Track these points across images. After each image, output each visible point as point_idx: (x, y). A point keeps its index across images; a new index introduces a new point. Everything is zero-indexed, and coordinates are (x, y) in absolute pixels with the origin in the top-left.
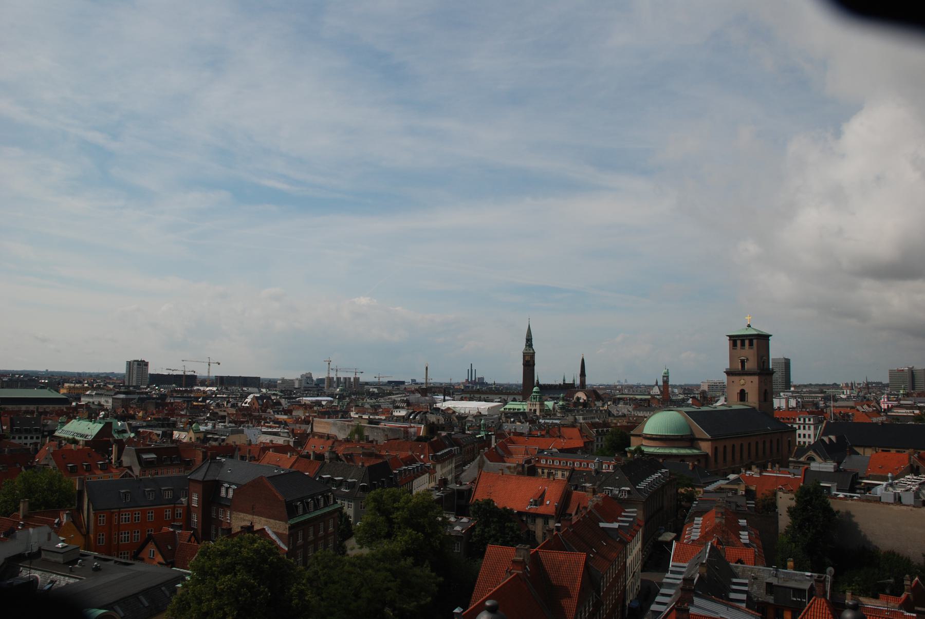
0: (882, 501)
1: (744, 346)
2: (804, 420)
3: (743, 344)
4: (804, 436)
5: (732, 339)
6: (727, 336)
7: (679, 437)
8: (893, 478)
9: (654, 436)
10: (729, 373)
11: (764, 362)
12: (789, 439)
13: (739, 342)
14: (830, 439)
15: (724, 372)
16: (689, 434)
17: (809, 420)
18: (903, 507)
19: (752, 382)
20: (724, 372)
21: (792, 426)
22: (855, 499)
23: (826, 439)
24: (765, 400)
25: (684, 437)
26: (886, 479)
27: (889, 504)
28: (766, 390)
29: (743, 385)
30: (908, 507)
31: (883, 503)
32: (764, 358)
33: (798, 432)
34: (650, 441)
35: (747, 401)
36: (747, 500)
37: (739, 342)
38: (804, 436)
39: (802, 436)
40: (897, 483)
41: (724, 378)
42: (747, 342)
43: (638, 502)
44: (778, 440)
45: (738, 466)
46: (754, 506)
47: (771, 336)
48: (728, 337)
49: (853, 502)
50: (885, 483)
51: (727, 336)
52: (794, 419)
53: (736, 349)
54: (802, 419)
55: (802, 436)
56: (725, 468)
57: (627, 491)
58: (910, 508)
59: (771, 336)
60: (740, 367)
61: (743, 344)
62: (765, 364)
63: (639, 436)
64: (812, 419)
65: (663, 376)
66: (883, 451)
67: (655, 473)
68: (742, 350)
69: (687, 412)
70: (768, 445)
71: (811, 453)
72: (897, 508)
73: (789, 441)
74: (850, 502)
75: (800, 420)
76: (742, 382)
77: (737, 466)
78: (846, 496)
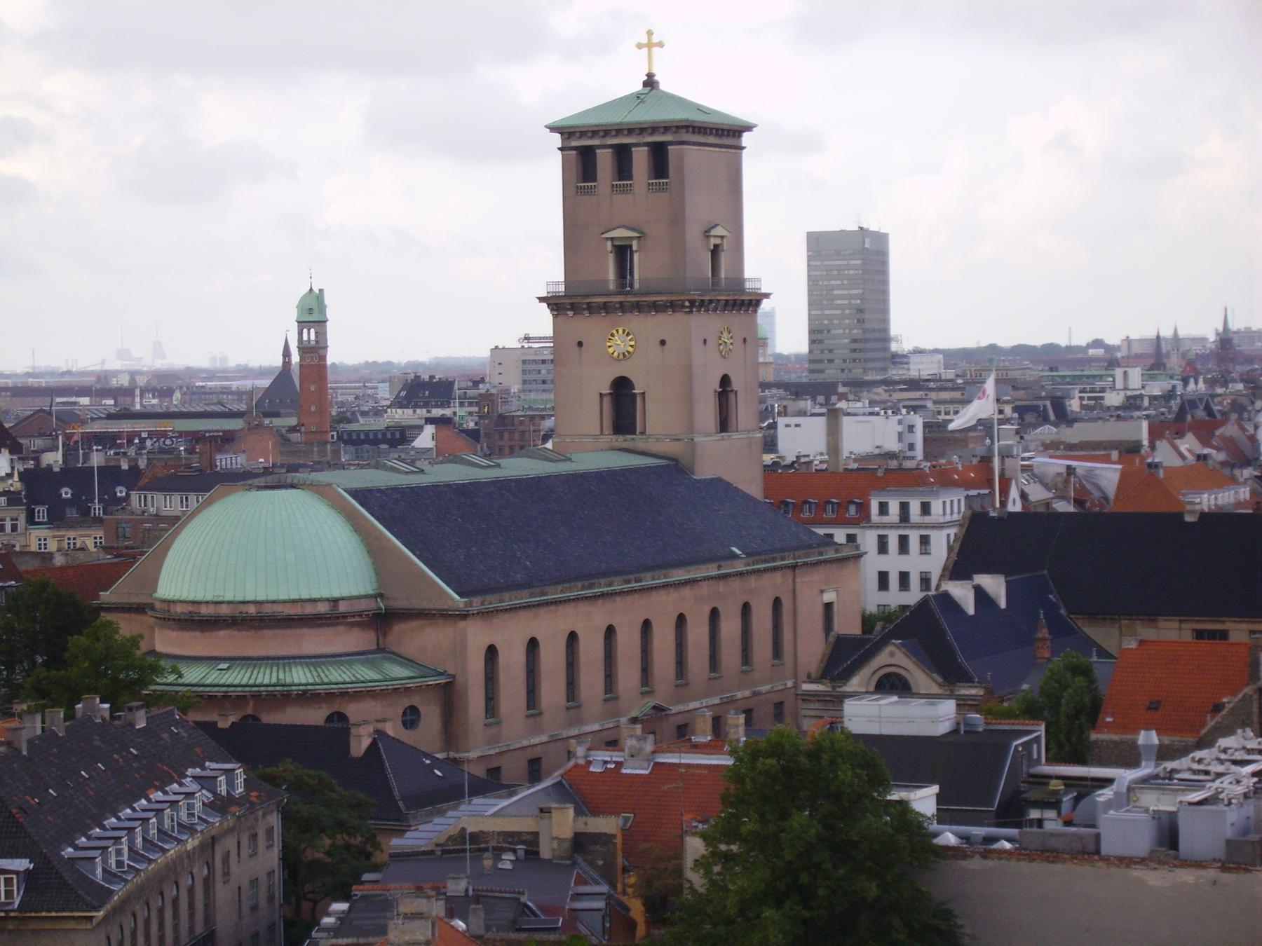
0: (1106, 849)
1: (630, 178)
2: (904, 507)
3: (623, 166)
4: (904, 578)
5: (574, 143)
6: (553, 129)
7: (322, 608)
8: (1164, 753)
9: (204, 610)
10: (555, 304)
11: (715, 251)
12: (829, 597)
13: (605, 160)
14: (981, 595)
15: (541, 300)
16: (371, 592)
17: (926, 508)
18: (1188, 876)
19: (663, 343)
20: (541, 300)
21: (851, 538)
22: (1005, 851)
23: (962, 593)
24: (724, 424)
25: (343, 607)
26: (1130, 758)
27: (1126, 861)
28: (725, 381)
29: (625, 356)
30: (1201, 872)
31: (1106, 860)
32: (719, 231)
33: (873, 563)
34: (187, 635)
35: (643, 433)
36: (580, 881)
37: (605, 160)
38: (904, 578)
39: (894, 581)
40: (1174, 771)
41: (542, 323)
42: (641, 159)
43: (71, 925)
44: (777, 603)
45: (596, 727)
46: (600, 904)
47: (749, 128)
48: (557, 139)
49: (990, 863)
50: (1125, 776)
51: (553, 129)
52: (864, 508)
53: (589, 192)
54: (894, 508)
55: (894, 581)
56: (536, 740)
57: (17, 873)
58: (1211, 874)
59: (749, 128)
60: (611, 275)
61: (623, 166)
62: (724, 258)
63: (140, 609)
64: (936, 507)
65: (302, 324)
66: (1199, 635)
67: (172, 781)
68: (620, 199)
69: (355, 494)
70: (730, 627)
71: (893, 657)
72: (1155, 878)
73: (828, 607)
74: (975, 864)
75: (883, 509)
76: (620, 343)
77: (588, 729)
78: (966, 838)
